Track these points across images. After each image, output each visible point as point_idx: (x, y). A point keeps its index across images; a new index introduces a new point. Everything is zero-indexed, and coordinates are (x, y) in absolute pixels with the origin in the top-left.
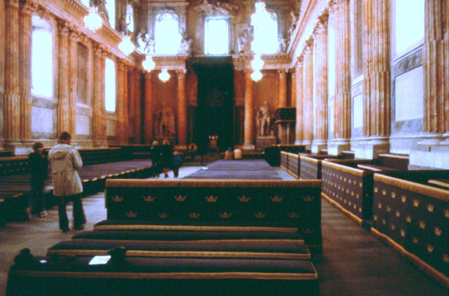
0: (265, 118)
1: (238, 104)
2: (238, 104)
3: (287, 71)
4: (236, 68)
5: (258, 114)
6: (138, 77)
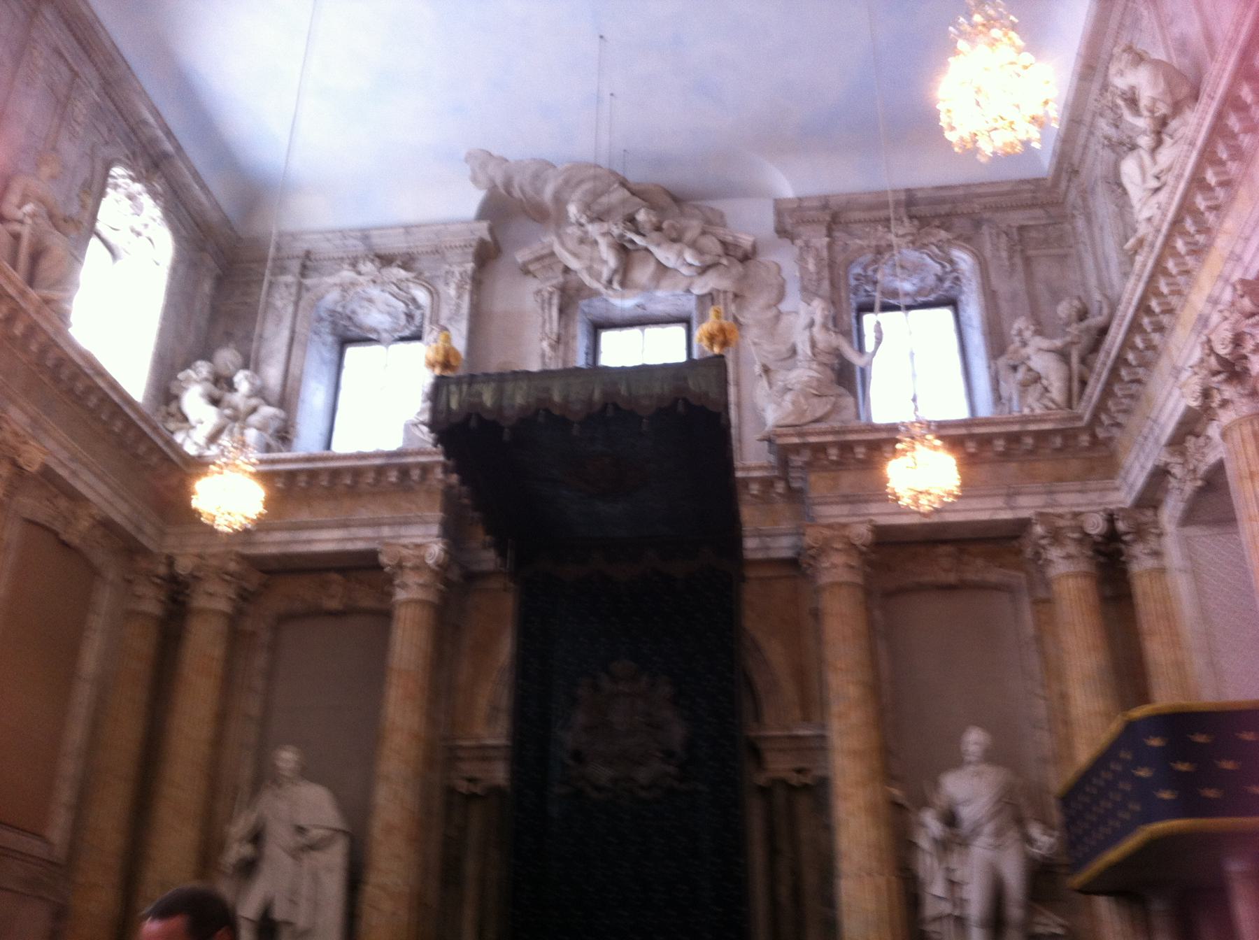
0: (980, 851)
1: (780, 765)
2: (780, 765)
3: (1095, 525)
4: (750, 543)
5: (932, 824)
6: (151, 603)
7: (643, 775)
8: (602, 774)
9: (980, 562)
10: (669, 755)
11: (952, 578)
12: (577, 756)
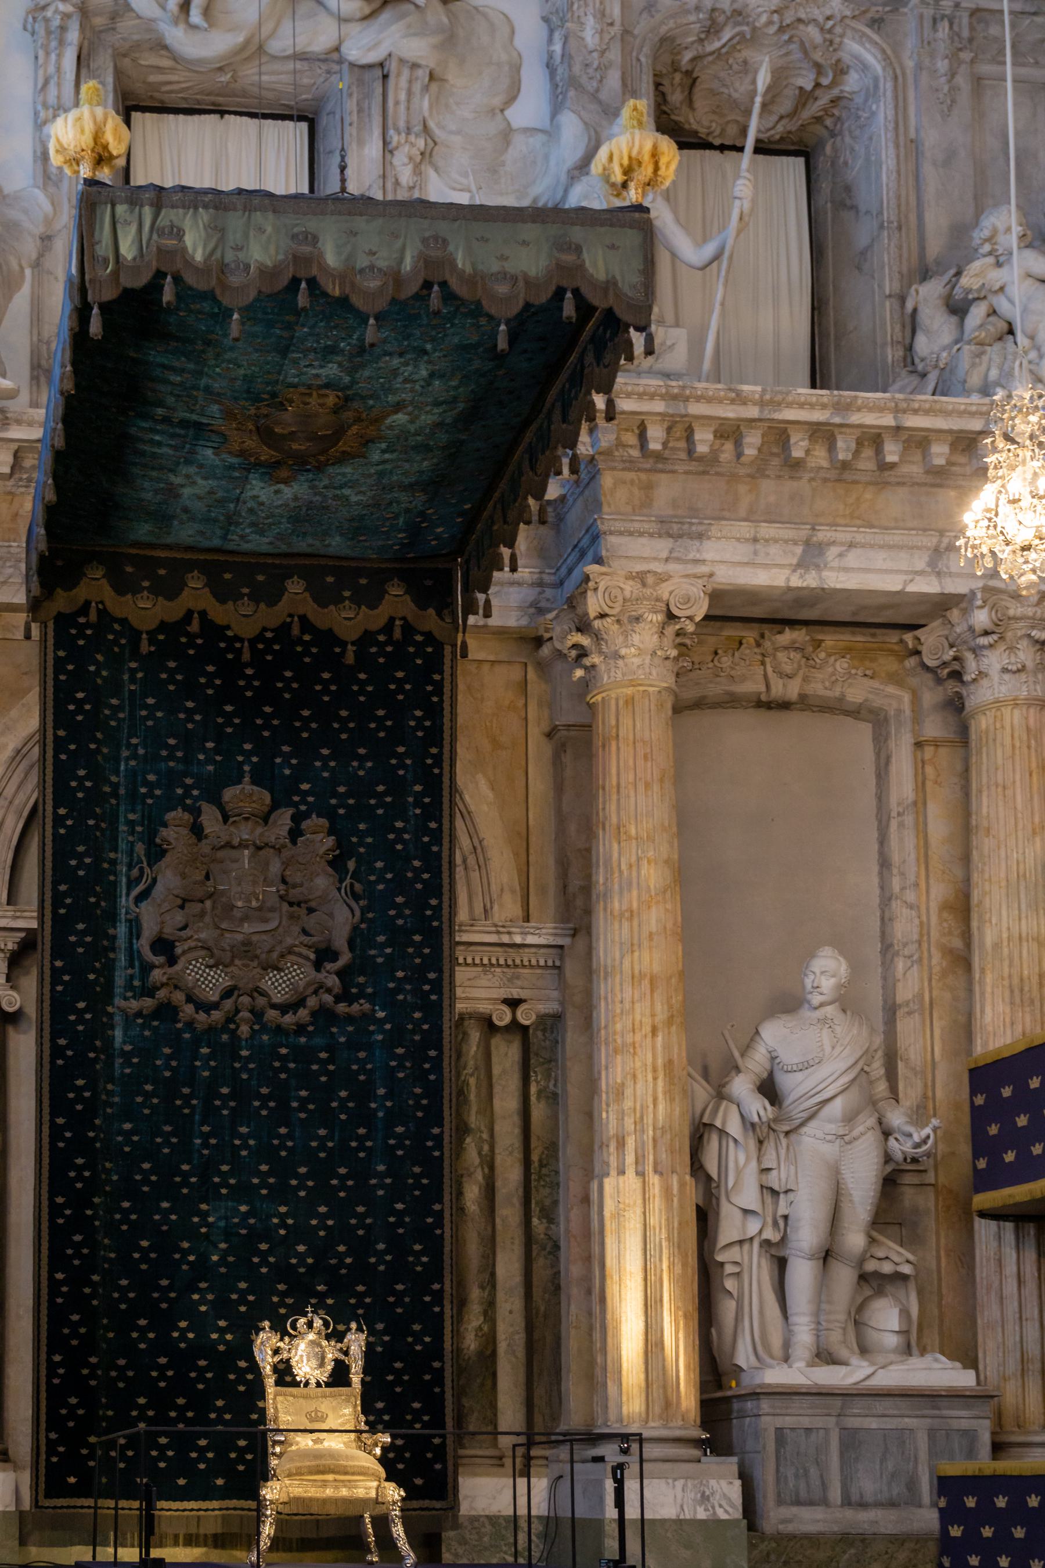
0: (816, 1142)
1: (476, 990)
7: (278, 987)
8: (210, 982)
9: (841, 665)
10: (324, 955)
11: (792, 690)
12: (164, 946)
